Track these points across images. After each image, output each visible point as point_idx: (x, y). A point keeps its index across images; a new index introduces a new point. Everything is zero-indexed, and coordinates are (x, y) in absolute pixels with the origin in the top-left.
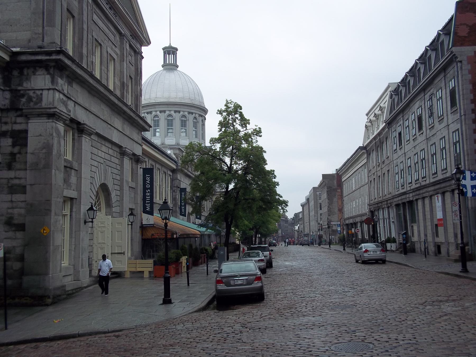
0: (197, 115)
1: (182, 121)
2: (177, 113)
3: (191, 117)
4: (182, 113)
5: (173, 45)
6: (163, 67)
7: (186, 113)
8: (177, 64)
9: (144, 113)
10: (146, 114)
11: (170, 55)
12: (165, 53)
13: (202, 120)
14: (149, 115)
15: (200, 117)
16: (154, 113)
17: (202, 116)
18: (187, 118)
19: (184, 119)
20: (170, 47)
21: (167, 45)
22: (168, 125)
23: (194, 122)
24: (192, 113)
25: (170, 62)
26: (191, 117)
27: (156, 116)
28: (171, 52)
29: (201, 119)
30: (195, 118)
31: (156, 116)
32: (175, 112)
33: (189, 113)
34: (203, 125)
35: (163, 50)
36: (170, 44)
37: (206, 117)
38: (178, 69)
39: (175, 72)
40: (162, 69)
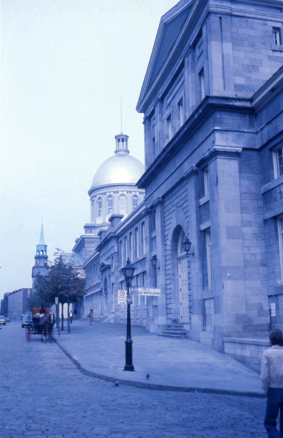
1: (134, 200)
2: (129, 194)
4: (133, 193)
5: (125, 133)
8: (129, 149)
10: (101, 195)
14: (104, 195)
18: (139, 198)
19: (135, 198)
21: (119, 133)
27: (110, 196)
31: (110, 196)
32: (128, 192)
36: (122, 133)
38: (129, 154)
40: (115, 154)
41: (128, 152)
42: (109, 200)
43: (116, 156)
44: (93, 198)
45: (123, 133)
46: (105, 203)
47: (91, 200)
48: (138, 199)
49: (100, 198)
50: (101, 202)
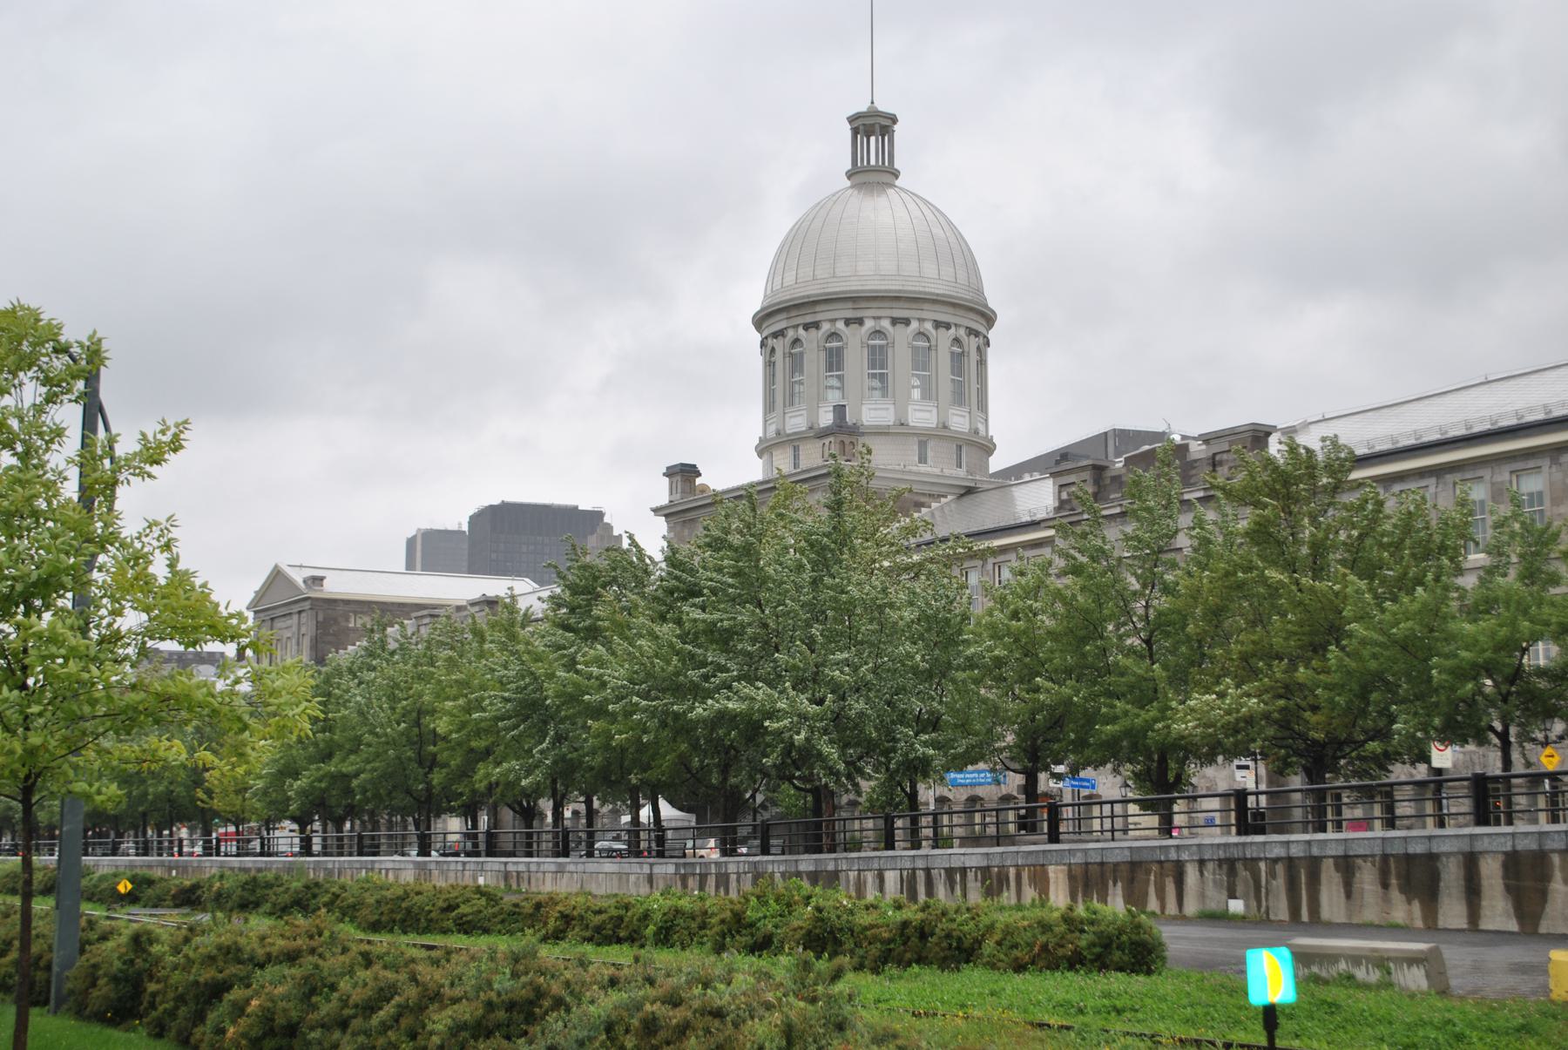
0: (962, 332)
1: (915, 349)
3: (944, 339)
4: (914, 325)
5: (882, 106)
6: (849, 178)
7: (929, 326)
9: (796, 327)
10: (801, 331)
11: (873, 139)
12: (855, 132)
13: (978, 348)
14: (813, 331)
15: (972, 337)
16: (826, 327)
17: (977, 334)
20: (873, 113)
21: (863, 107)
22: (872, 365)
23: (952, 353)
24: (948, 326)
25: (873, 162)
26: (944, 339)
27: (834, 335)
28: (877, 127)
29: (973, 342)
30: (957, 341)
31: (834, 335)
33: (938, 325)
34: (982, 363)
35: (850, 122)
37: (991, 335)
38: (898, 183)
39: (890, 191)
40: (848, 183)
41: (896, 174)
42: (831, 349)
43: (852, 187)
44: (770, 342)
45: (876, 104)
46: (814, 359)
47: (763, 345)
48: (929, 348)
49: (796, 341)
50: (801, 354)
